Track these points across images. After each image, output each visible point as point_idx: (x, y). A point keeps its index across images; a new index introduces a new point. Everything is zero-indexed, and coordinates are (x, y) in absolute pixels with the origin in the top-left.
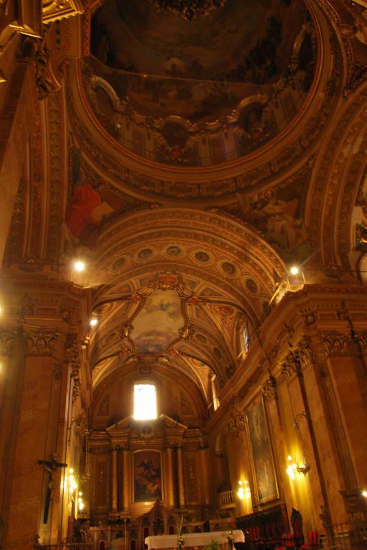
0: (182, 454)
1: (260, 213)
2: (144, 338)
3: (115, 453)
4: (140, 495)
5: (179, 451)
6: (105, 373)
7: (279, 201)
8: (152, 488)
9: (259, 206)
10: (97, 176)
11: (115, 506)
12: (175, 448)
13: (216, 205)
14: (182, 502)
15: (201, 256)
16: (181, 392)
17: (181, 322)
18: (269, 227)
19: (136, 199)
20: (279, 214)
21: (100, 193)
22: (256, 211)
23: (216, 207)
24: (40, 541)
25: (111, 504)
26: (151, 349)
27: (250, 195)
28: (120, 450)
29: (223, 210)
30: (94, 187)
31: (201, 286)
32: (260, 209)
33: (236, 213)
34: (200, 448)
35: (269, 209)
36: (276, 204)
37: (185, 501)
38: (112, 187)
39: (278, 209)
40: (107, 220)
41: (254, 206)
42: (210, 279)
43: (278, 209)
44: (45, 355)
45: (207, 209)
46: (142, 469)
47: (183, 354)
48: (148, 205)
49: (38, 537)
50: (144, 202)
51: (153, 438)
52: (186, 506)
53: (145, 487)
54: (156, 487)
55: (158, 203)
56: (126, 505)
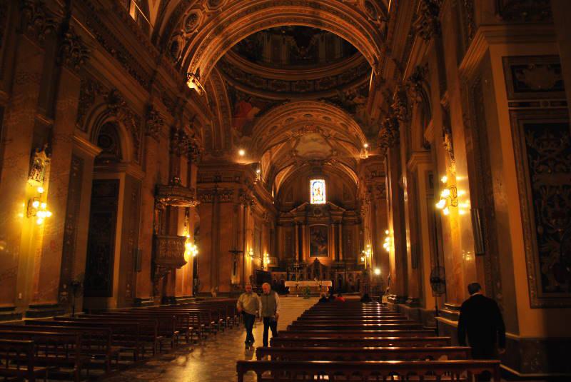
0: (342, 228)
1: (351, 102)
2: (308, 154)
3: (297, 227)
4: (314, 252)
5: (340, 226)
6: (288, 174)
7: (362, 96)
8: (322, 249)
9: (350, 98)
10: (247, 95)
11: (297, 259)
12: (337, 224)
13: (326, 96)
14: (341, 258)
15: (325, 118)
16: (344, 185)
17: (329, 148)
18: (357, 111)
19: (272, 100)
20: (363, 104)
21: (251, 103)
22: (348, 101)
23: (325, 99)
24: (233, 282)
25: (295, 257)
26: (317, 159)
27: (344, 91)
28: (300, 225)
29: (328, 100)
30: (246, 101)
31: (333, 132)
32: (351, 100)
33: (338, 103)
34: (356, 223)
35: (356, 100)
36: (360, 98)
37: (343, 256)
38: (257, 97)
39: (361, 101)
40: (258, 116)
41: (348, 98)
42: (335, 130)
43: (361, 101)
44: (229, 202)
45: (319, 100)
46: (315, 237)
47: (339, 162)
48: (281, 102)
49: (231, 281)
50: (279, 101)
51: (321, 217)
52: (343, 260)
53: (317, 248)
54: (324, 247)
55: (286, 100)
56: (304, 259)
